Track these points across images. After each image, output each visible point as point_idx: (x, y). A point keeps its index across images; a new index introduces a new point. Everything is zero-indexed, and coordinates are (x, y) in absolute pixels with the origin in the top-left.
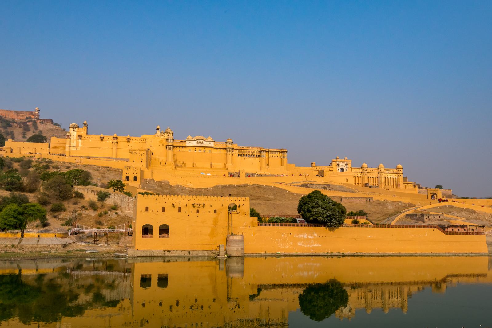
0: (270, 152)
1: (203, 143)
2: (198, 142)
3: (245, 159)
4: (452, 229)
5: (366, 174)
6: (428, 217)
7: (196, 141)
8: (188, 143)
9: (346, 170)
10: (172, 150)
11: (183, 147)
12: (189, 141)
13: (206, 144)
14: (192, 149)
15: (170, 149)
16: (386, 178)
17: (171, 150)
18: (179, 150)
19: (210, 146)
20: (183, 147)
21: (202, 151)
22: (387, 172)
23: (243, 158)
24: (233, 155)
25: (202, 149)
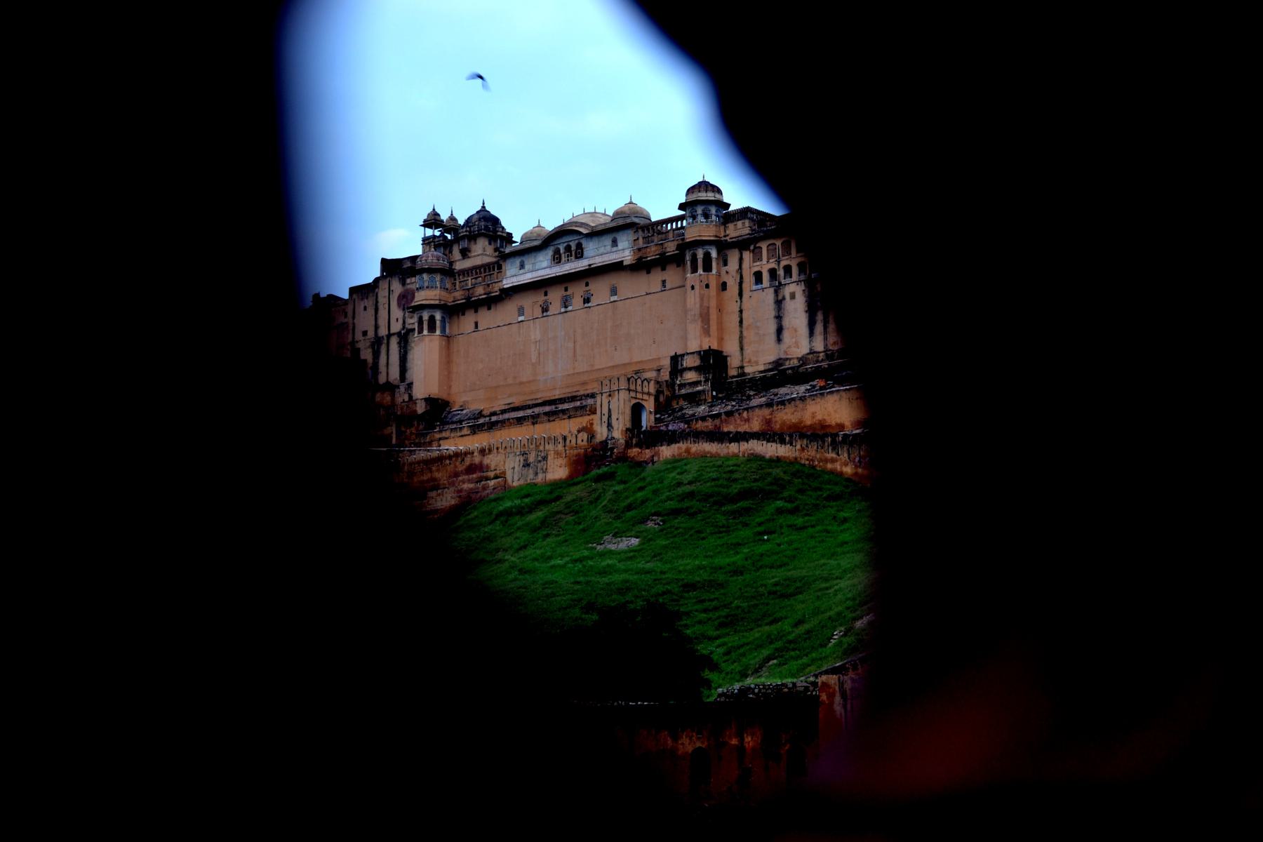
1: (579, 254)
2: (557, 252)
3: (793, 296)
7: (549, 253)
8: (513, 276)
10: (432, 328)
12: (518, 261)
13: (597, 254)
14: (530, 302)
15: (421, 331)
17: (425, 332)
18: (476, 324)
19: (612, 258)
20: (491, 302)
21: (577, 302)
24: (724, 286)
25: (577, 291)
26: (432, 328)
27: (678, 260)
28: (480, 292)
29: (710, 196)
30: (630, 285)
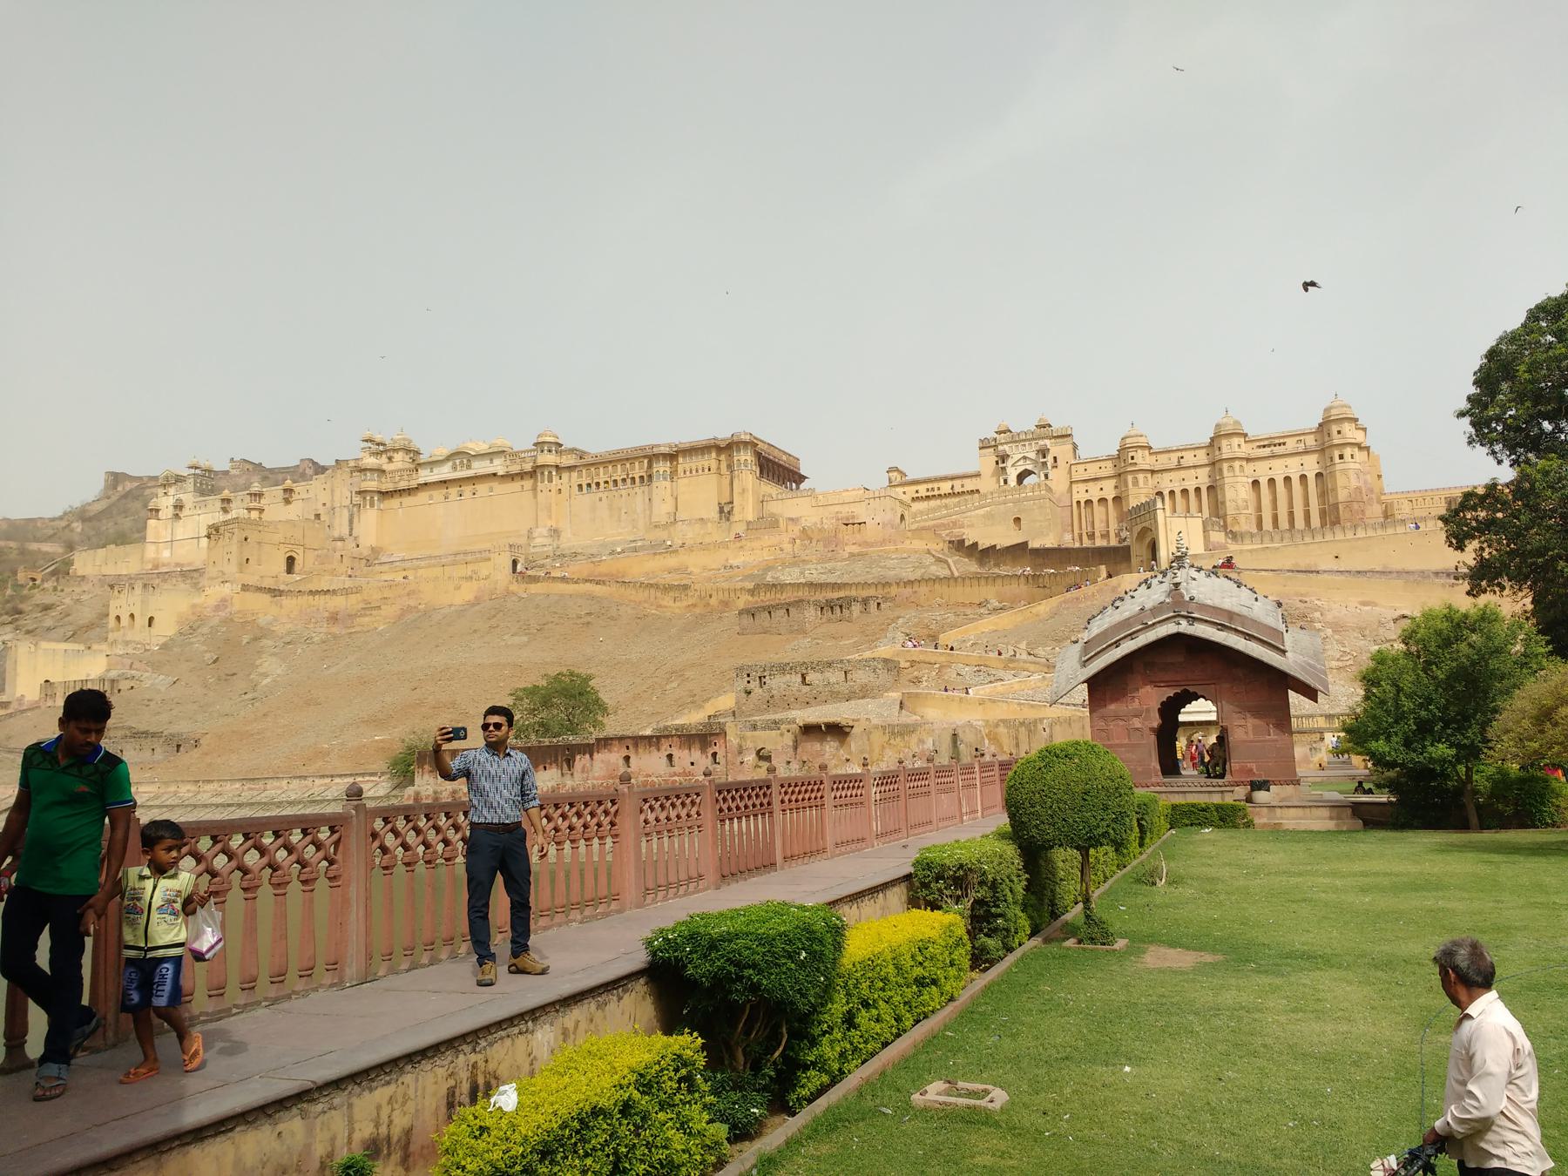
0: (681, 460)
1: (469, 467)
4: (625, 752)
5: (1136, 483)
6: (763, 683)
7: (450, 464)
8: (425, 476)
9: (1046, 476)
10: (372, 505)
11: (409, 491)
13: (480, 467)
14: (438, 494)
16: (1264, 482)
19: (491, 470)
20: (409, 491)
22: (1267, 452)
23: (595, 496)
25: (467, 489)
26: (372, 505)
27: (532, 474)
28: (403, 485)
29: (552, 439)
30: (498, 488)
